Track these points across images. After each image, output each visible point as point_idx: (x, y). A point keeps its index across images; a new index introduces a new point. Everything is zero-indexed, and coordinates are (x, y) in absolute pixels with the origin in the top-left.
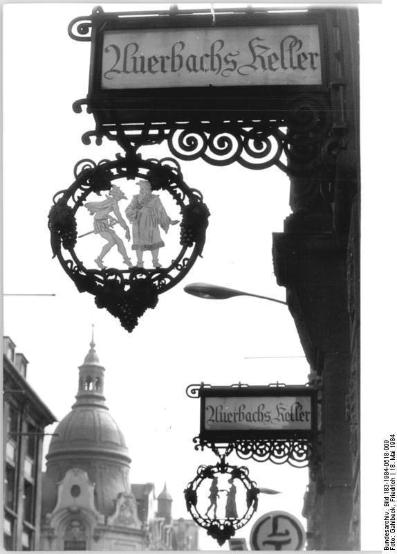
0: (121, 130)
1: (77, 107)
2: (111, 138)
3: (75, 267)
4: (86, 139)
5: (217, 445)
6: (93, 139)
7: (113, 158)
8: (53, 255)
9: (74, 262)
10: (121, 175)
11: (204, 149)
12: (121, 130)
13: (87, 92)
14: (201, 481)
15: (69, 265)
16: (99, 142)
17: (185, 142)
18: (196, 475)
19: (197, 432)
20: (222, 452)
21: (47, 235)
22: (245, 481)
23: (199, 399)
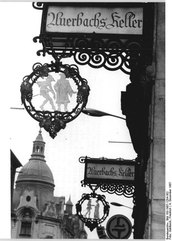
0: (53, 50)
1: (35, 40)
2: (49, 53)
3: (31, 109)
4: (38, 54)
5: (91, 185)
6: (42, 53)
7: (50, 63)
9: (31, 107)
10: (53, 70)
11: (89, 60)
12: (53, 50)
13: (39, 34)
14: (83, 201)
15: (29, 108)
16: (44, 55)
17: (81, 57)
18: (81, 198)
19: (83, 179)
20: (94, 188)
21: (19, 94)
22: (103, 202)
23: (84, 164)
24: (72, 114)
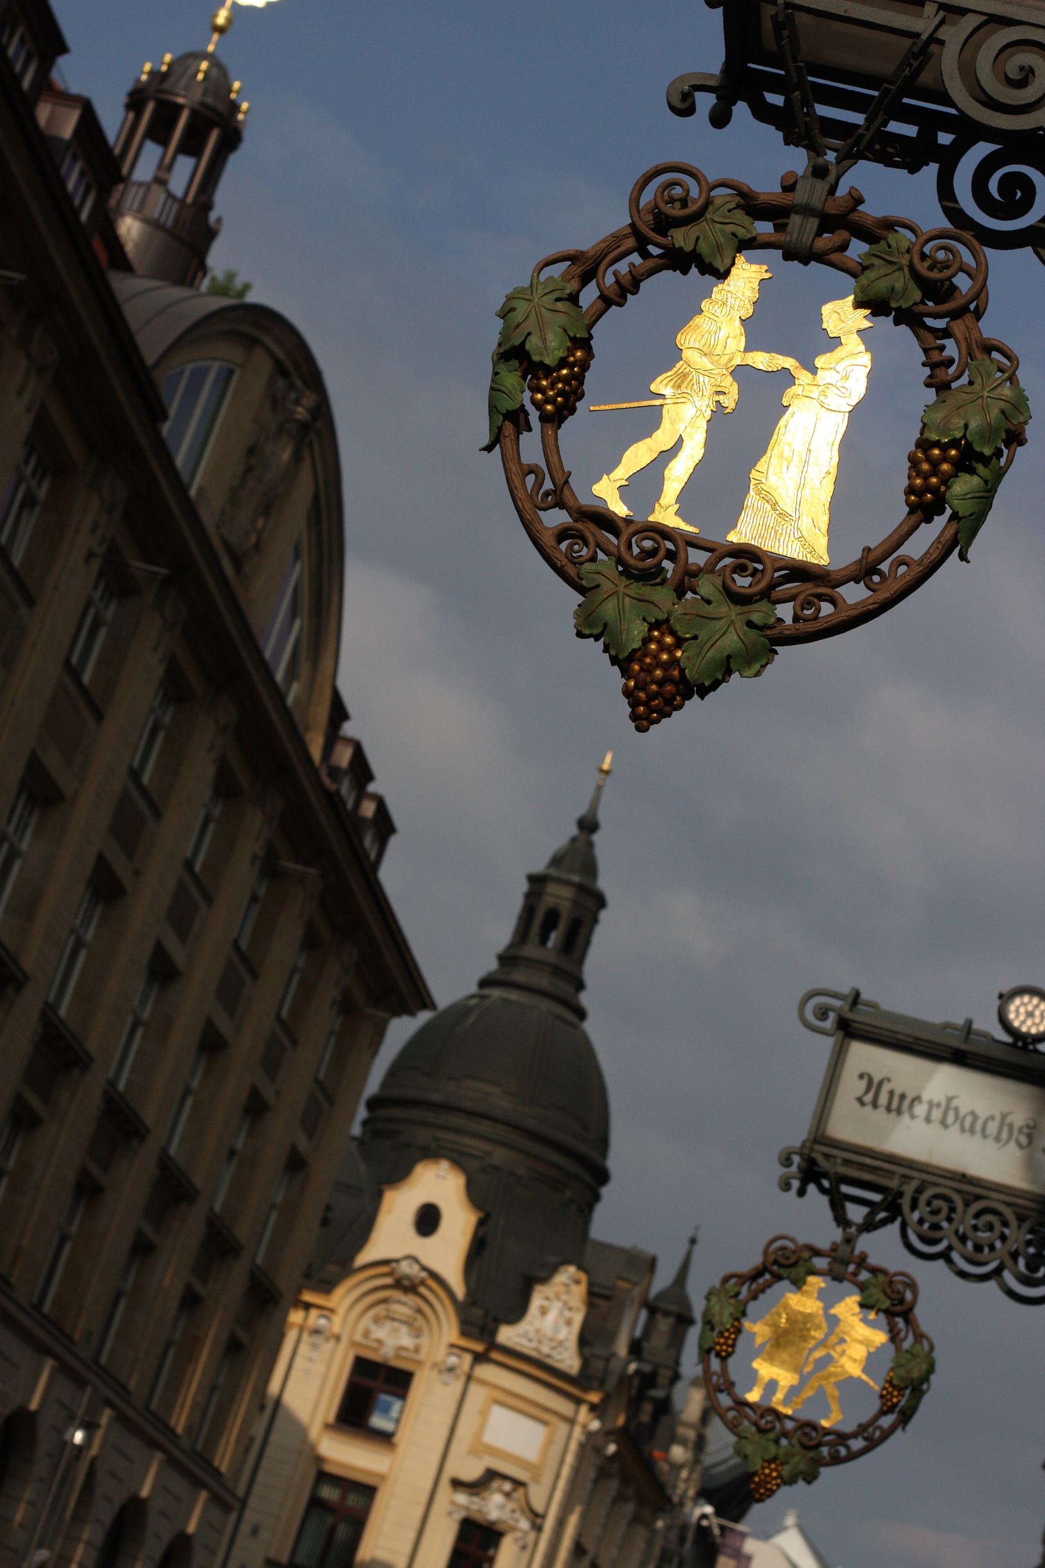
3: (547, 494)
6: (705, 101)
8: (486, 441)
14: (769, 1285)
16: (720, 119)
22: (900, 1322)
24: (842, 590)
